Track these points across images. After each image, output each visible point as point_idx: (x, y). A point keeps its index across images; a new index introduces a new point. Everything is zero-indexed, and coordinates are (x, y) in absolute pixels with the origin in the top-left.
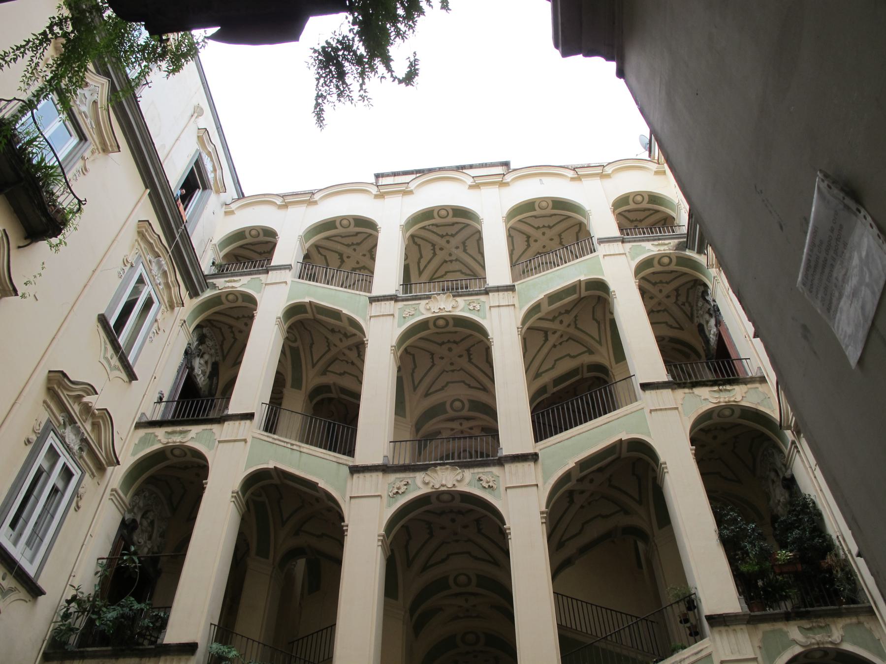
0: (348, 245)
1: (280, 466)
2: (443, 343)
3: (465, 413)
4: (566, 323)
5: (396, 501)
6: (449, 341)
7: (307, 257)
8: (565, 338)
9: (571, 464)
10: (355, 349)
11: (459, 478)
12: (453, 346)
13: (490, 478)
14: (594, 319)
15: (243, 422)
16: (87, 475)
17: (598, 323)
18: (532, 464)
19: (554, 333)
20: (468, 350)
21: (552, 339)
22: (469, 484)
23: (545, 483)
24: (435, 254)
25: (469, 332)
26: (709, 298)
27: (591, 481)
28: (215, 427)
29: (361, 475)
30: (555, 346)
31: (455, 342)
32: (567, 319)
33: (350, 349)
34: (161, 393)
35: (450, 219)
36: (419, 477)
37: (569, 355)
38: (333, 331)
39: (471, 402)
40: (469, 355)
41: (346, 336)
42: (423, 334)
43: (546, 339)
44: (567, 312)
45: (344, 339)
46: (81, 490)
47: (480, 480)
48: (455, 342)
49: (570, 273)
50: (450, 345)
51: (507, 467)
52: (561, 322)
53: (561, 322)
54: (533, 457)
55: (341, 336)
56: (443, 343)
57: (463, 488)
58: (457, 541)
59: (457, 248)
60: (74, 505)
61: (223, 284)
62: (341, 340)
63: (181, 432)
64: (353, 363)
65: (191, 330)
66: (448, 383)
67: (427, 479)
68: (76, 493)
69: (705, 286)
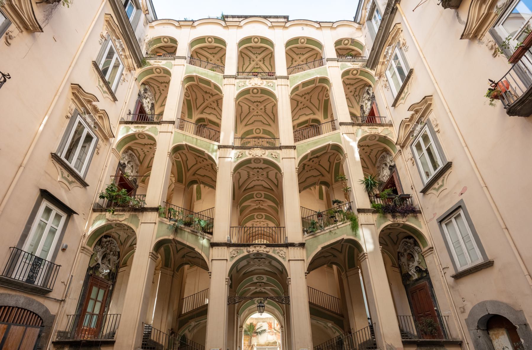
0: (211, 54)
1: (187, 143)
2: (255, 102)
3: (261, 135)
4: (306, 99)
5: (238, 160)
6: (257, 102)
7: (192, 56)
8: (305, 106)
9: (309, 151)
10: (216, 103)
11: (263, 153)
12: (259, 104)
13: (276, 154)
14: (318, 99)
15: (170, 125)
16: (100, 140)
17: (319, 101)
18: (293, 150)
19: (301, 103)
20: (265, 106)
21: (300, 106)
22: (267, 156)
23: (298, 157)
24: (250, 63)
25: (266, 97)
26: (371, 92)
27: (313, 161)
28: (157, 126)
29: (223, 149)
30: (300, 109)
31: (259, 102)
32: (308, 97)
33: (214, 102)
34: (130, 110)
35: (259, 44)
36: (247, 152)
37: (305, 114)
38: (206, 92)
39: (263, 130)
40: (265, 109)
41: (212, 95)
42: (247, 96)
43: (297, 105)
44: (308, 93)
45: (211, 96)
46: (98, 146)
47: (272, 154)
48: (259, 102)
49: (312, 73)
50: (257, 103)
51: (283, 150)
52: (305, 98)
53: (305, 98)
54: (294, 147)
55: (210, 95)
56: (255, 102)
57: (264, 157)
58: (258, 180)
59: (260, 61)
60: (96, 151)
61: (154, 63)
62: (210, 97)
63: (142, 127)
64: (215, 109)
65: (140, 83)
66: (255, 121)
67: (250, 152)
68: (95, 147)
69: (370, 86)
